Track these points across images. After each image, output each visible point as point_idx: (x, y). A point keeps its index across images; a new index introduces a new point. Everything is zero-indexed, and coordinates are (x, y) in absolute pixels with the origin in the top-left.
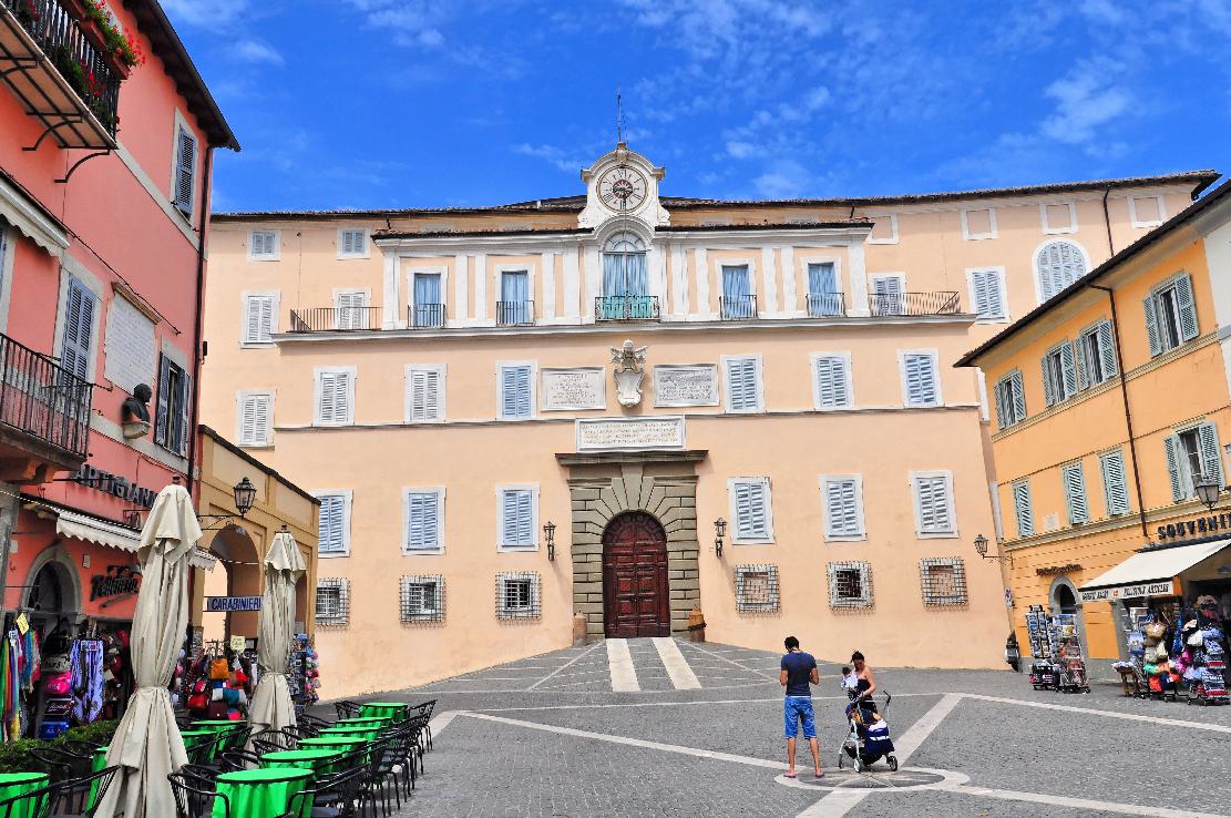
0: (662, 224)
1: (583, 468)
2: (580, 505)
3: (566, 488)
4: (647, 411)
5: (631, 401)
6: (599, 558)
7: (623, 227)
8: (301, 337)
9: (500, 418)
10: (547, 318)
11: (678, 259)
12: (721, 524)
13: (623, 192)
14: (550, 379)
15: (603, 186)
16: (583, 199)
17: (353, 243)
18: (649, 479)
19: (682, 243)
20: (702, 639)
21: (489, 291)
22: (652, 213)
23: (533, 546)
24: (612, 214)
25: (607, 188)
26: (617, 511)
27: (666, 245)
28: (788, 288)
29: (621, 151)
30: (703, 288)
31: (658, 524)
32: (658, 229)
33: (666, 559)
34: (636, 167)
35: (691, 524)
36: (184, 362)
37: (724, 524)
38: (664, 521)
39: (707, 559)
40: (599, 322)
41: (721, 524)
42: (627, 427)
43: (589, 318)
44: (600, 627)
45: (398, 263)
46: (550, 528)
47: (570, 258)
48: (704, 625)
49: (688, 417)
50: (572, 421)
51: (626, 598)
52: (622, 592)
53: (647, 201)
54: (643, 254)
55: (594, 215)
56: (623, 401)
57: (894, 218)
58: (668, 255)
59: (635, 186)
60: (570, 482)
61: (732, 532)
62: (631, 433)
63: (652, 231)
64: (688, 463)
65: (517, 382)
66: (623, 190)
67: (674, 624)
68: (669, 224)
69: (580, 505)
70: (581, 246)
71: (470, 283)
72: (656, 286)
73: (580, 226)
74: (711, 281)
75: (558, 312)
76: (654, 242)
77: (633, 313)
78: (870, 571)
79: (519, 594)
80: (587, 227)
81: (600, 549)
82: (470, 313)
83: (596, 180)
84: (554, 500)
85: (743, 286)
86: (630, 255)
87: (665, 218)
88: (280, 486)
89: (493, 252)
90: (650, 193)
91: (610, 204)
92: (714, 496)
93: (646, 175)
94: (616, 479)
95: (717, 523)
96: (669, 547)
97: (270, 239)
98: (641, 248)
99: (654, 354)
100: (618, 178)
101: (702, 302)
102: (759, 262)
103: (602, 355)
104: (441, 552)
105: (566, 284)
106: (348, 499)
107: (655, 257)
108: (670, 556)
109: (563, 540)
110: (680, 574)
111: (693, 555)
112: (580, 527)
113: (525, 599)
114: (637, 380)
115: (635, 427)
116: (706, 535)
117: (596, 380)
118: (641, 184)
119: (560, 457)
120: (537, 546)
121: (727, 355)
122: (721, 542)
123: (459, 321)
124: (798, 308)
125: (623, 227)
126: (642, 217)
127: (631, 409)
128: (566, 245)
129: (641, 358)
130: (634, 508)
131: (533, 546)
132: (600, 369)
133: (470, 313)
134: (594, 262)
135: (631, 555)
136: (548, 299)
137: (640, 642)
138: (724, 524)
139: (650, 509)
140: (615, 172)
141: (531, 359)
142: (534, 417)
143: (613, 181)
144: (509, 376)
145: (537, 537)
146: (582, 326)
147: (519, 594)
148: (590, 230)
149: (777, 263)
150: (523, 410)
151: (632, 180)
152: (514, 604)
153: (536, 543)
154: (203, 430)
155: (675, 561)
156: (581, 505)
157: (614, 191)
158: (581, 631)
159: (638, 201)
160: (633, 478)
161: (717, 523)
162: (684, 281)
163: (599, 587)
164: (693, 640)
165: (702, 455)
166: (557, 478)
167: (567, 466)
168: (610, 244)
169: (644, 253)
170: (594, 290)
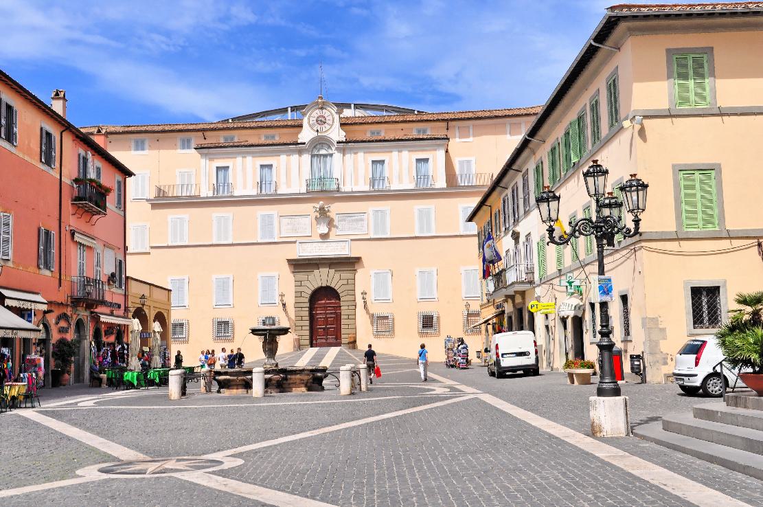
1: (299, 265)
2: (299, 283)
3: (292, 275)
4: (332, 237)
6: (307, 309)
7: (321, 141)
8: (162, 201)
9: (260, 241)
10: (283, 190)
11: (349, 157)
13: (321, 121)
14: (285, 221)
15: (311, 119)
16: (301, 126)
17: (186, 144)
18: (332, 271)
19: (351, 149)
21: (254, 174)
22: (337, 134)
25: (313, 120)
26: (316, 287)
27: (343, 151)
28: (405, 172)
29: (320, 101)
30: (361, 172)
31: (337, 293)
35: (352, 292)
36: (121, 257)
40: (308, 192)
41: (364, 293)
42: (319, 244)
43: (304, 190)
44: (308, 342)
45: (207, 161)
46: (282, 295)
47: (295, 157)
49: (352, 240)
50: (295, 242)
51: (321, 328)
53: (333, 127)
54: (331, 155)
55: (306, 135)
57: (471, 127)
61: (371, 298)
63: (335, 144)
64: (349, 263)
65: (267, 222)
66: (321, 121)
67: (344, 341)
69: (299, 283)
70: (300, 152)
71: (244, 173)
76: (337, 149)
78: (438, 318)
80: (303, 141)
81: (308, 305)
82: (245, 187)
83: (307, 116)
86: (325, 156)
88: (155, 288)
89: (254, 154)
90: (335, 121)
92: (364, 279)
93: (333, 112)
94: (316, 271)
96: (342, 304)
97: (143, 142)
98: (330, 152)
99: (335, 209)
101: (361, 181)
103: (310, 208)
104: (232, 306)
105: (292, 172)
106: (187, 281)
107: (337, 156)
109: (290, 301)
112: (299, 294)
115: (325, 245)
117: (307, 221)
118: (331, 118)
119: (289, 261)
123: (238, 192)
124: (411, 183)
125: (321, 141)
126: (330, 136)
127: (324, 237)
128: (293, 152)
129: (328, 211)
133: (245, 187)
134: (306, 158)
136: (283, 179)
139: (333, 286)
140: (317, 111)
141: (273, 210)
143: (316, 116)
145: (277, 300)
148: (304, 143)
149: (400, 161)
151: (326, 116)
153: (277, 302)
154: (127, 278)
155: (344, 311)
156: (299, 283)
157: (317, 121)
159: (328, 127)
160: (324, 271)
162: (351, 170)
163: (307, 323)
164: (350, 348)
165: (358, 259)
166: (287, 269)
168: (315, 150)
169: (331, 155)
170: (306, 174)
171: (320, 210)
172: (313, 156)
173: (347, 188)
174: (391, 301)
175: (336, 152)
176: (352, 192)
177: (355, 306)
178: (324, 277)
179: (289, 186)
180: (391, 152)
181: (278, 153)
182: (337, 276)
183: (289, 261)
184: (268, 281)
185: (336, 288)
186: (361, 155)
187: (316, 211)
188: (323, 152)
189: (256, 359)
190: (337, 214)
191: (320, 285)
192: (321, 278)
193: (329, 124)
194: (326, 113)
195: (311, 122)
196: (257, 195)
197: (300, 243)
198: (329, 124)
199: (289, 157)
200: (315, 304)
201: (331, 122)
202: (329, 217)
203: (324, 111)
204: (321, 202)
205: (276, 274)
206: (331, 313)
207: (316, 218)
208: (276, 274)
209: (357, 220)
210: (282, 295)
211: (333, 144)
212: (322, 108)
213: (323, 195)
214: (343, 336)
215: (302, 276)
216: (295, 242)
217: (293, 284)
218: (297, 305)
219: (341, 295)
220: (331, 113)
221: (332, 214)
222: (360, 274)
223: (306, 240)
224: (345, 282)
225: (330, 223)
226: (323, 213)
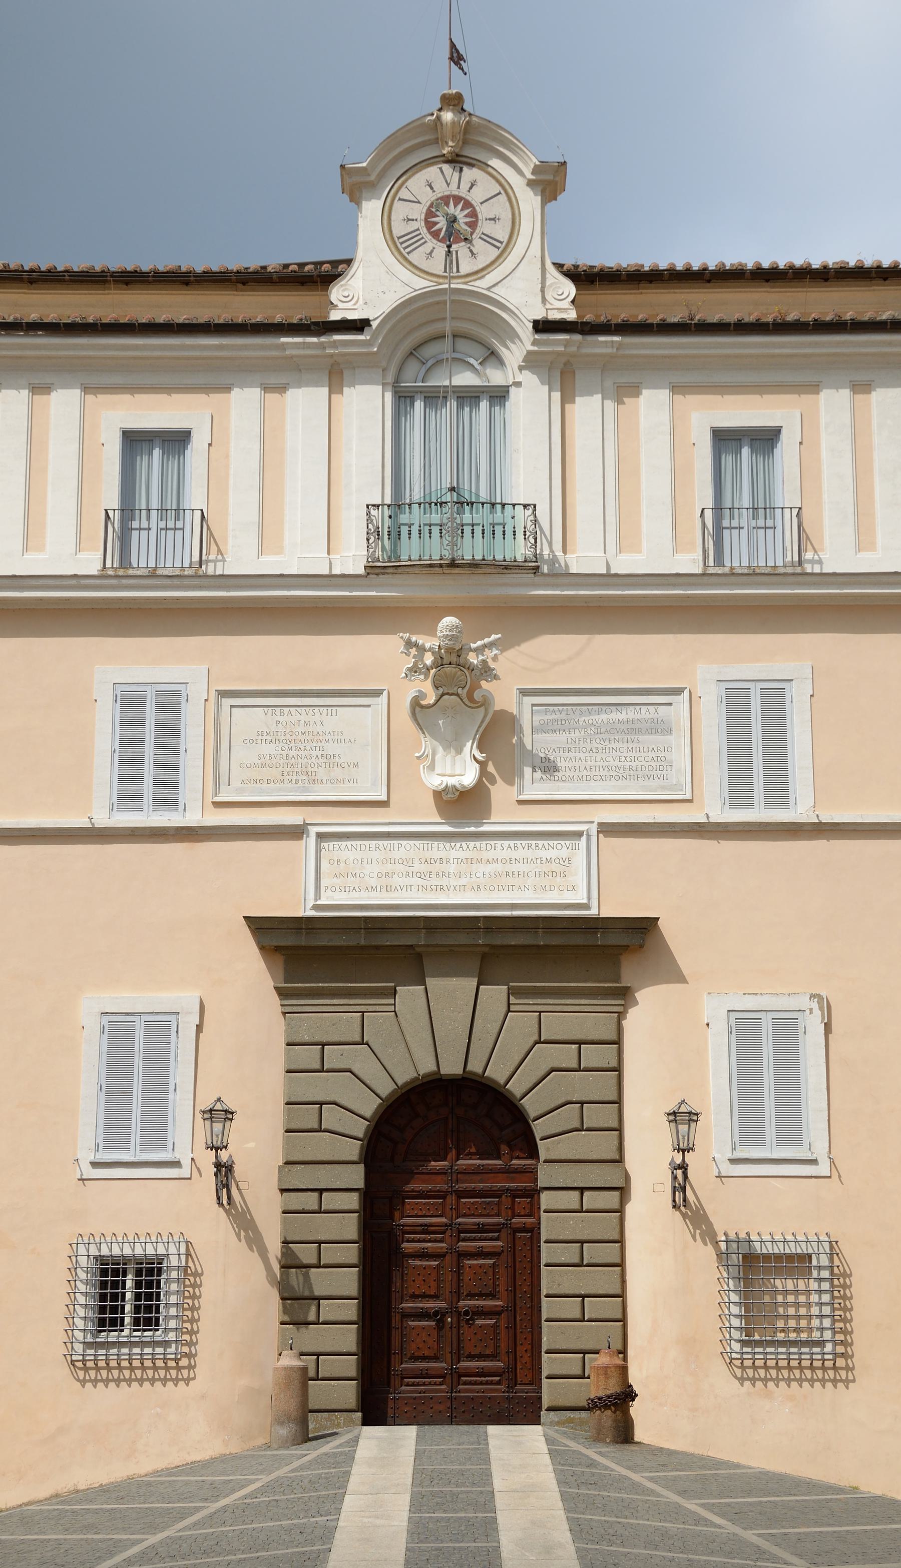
0: (554, 316)
2: (309, 1056)
5: (452, 781)
6: (353, 1201)
9: (103, 818)
12: (682, 1117)
14: (248, 720)
15: (400, 210)
20: (624, 1433)
23: (177, 1164)
24: (421, 284)
25: (409, 215)
26: (404, 1075)
27: (565, 378)
29: (448, 116)
32: (542, 327)
33: (534, 1210)
34: (495, 163)
37: (692, 1117)
38: (531, 1105)
39: (648, 1216)
40: (373, 570)
41: (682, 1117)
42: (438, 849)
43: (352, 557)
44: (348, 1393)
47: (305, 402)
48: (629, 1395)
50: (296, 832)
52: (414, 1297)
54: (499, 396)
56: (436, 781)
58: (567, 398)
59: (483, 212)
60: (282, 993)
61: (716, 1139)
62: (452, 868)
63: (526, 332)
68: (572, 315)
69: (309, 1056)
70: (336, 375)
72: (525, 477)
73: (335, 316)
74: (678, 474)
75: (267, 536)
76: (531, 362)
77: (472, 548)
79: (128, 1297)
81: (356, 1176)
84: (240, 1043)
85: (763, 485)
86: (468, 397)
87: (562, 299)
89: (97, 381)
91: (416, 257)
93: (517, 183)
94: (409, 996)
95: (674, 1116)
96: (545, 1176)
98: (496, 377)
100: (441, 190)
102: (807, 422)
103: (384, 659)
105: (293, 472)
107: (531, 401)
108: (546, 1200)
109: (258, 1148)
110: (570, 1253)
111: (611, 1199)
112: (304, 1116)
113: (147, 1317)
114: (476, 719)
115: (459, 851)
116: (647, 1154)
117: (364, 723)
118: (500, 208)
119: (260, 927)
120: (186, 1162)
121: (709, 665)
122: (683, 1167)
127: (463, 806)
128: (296, 372)
129: (486, 671)
130: (452, 1067)
131: (177, 1164)
132: (377, 693)
135: (442, 1195)
137: (453, 1438)
138: (692, 1117)
139: (497, 1073)
140: (432, 172)
141: (184, 664)
142: (192, 817)
143: (427, 197)
144: (130, 703)
145: (186, 1139)
146: (331, 580)
147: (128, 1297)
148: (359, 326)
150: (167, 795)
151: (476, 197)
152: (113, 1322)
156: (308, 1059)
158: (292, 1405)
159: (486, 253)
160: (452, 991)
161: (674, 1116)
162: (608, 475)
164: (598, 1438)
165: (642, 930)
166: (251, 974)
167: (278, 949)
169: (499, 396)
170: (365, 480)
171: (439, 663)
172: (403, 398)
173: (587, 554)
174: (823, 1169)
175: (529, 378)
176: (610, 578)
177: (623, 1191)
178: (452, 1026)
179: (267, 536)
180: (814, 388)
181: (215, 380)
182: (522, 1025)
183: (260, 927)
184: (135, 1053)
185: (516, 1087)
186: (653, 405)
187: (414, 670)
188: (465, 379)
189: (43, 1491)
190: (524, 692)
191: (427, 1066)
192: (433, 1027)
193: (488, 239)
194: (475, 185)
195: (399, 229)
196: (102, 578)
197: (321, 836)
198: (488, 239)
199: (272, 397)
200: (410, 1175)
201: (501, 232)
202: (486, 703)
203: (469, 174)
204: (449, 621)
205: (183, 1000)
206: (482, 1229)
207: (417, 705)
208: (183, 1000)
209: (634, 729)
210: (217, 1114)
211: (513, 335)
212: (457, 160)
213: (456, 588)
214: (548, 1364)
215: (335, 1019)
216: (296, 832)
217: (277, 1058)
218: (298, 1186)
219: (539, 1128)
220: (505, 188)
221: (503, 694)
222: (649, 1018)
223: (363, 821)
224: (566, 1055)
225: (497, 738)
226: (456, 682)
